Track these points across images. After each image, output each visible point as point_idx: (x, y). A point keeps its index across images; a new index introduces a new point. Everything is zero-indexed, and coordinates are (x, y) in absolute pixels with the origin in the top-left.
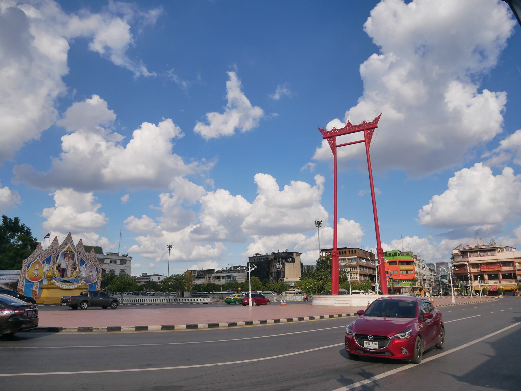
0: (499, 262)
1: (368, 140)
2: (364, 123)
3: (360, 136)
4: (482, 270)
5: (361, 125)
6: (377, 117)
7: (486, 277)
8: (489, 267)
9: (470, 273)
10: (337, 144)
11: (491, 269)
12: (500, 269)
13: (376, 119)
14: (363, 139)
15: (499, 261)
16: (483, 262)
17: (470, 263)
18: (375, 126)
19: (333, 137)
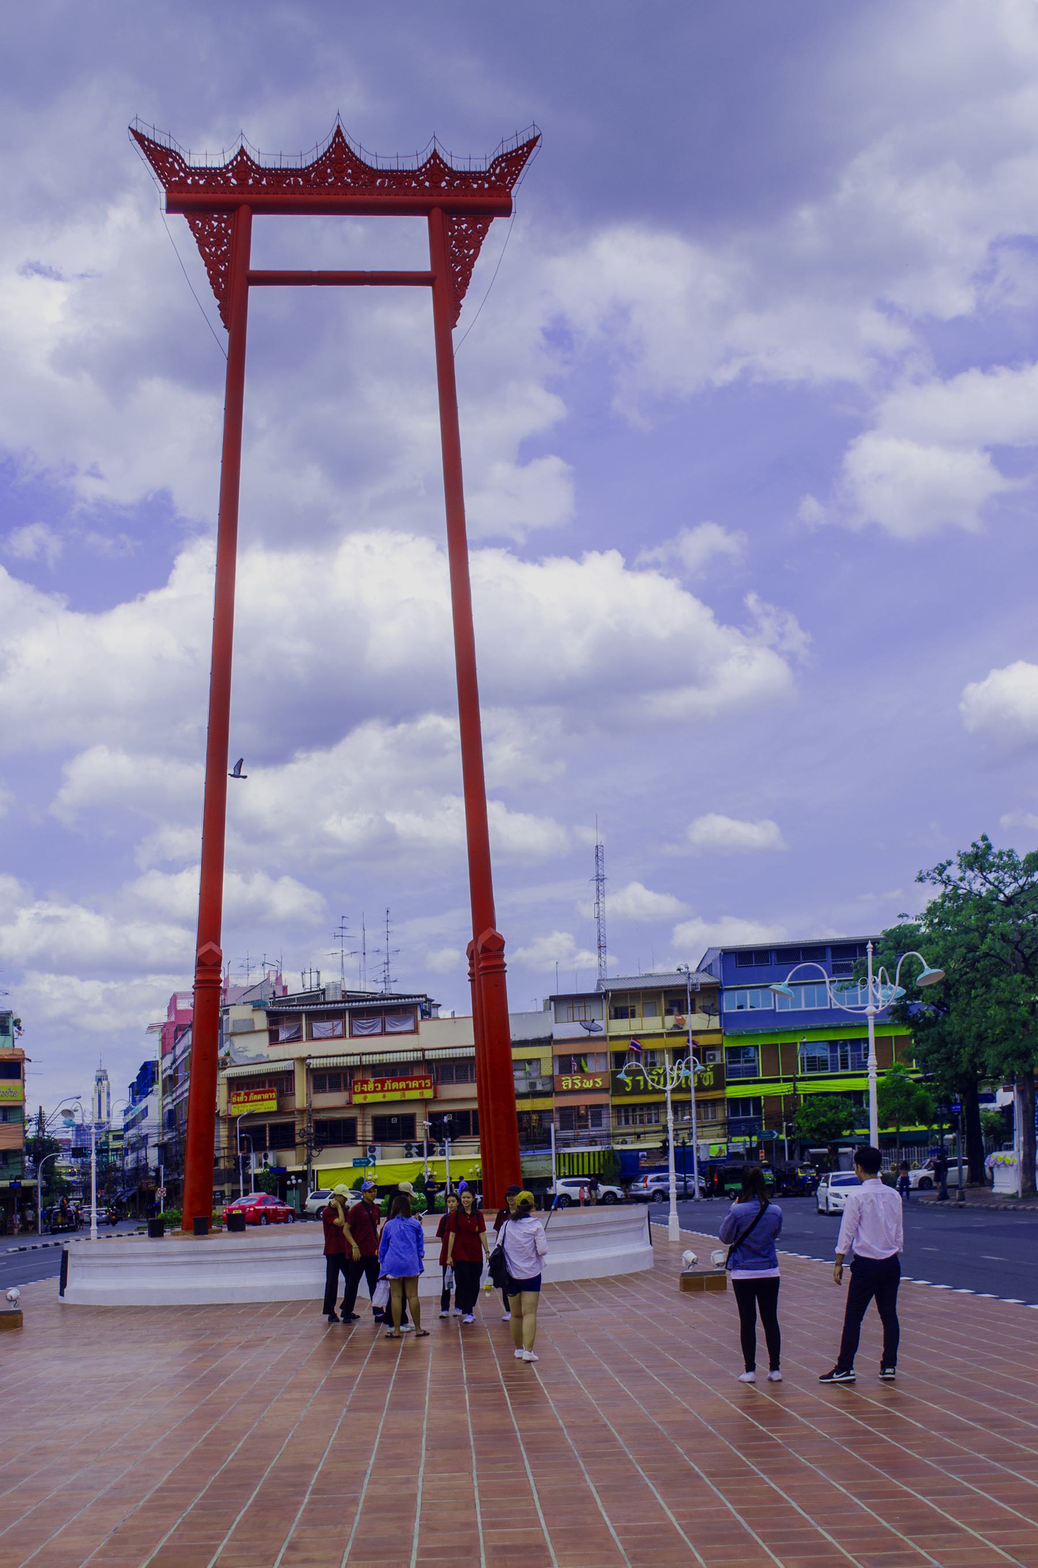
0: (429, 1062)
2: (436, 167)
3: (406, 241)
4: (358, 1099)
5: (412, 175)
7: (365, 1130)
9: (302, 1112)
10: (256, 263)
12: (428, 1094)
15: (429, 1055)
16: (367, 1060)
17: (314, 1063)
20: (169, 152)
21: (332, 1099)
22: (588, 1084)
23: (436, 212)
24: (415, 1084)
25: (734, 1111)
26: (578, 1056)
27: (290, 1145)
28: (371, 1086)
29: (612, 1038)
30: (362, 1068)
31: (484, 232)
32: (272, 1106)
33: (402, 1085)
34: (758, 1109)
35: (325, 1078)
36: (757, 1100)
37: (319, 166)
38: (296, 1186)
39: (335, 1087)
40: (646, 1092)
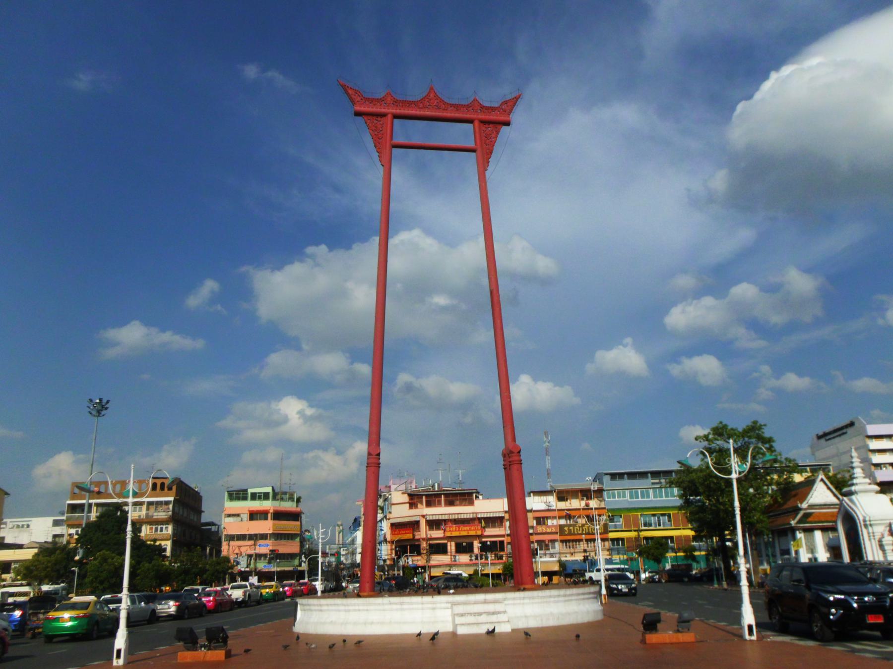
0: (480, 519)
1: (484, 151)
3: (463, 134)
4: (448, 534)
6: (509, 97)
7: (451, 547)
8: (462, 528)
9: (424, 539)
11: (464, 531)
12: (479, 533)
13: (506, 102)
14: (471, 144)
15: (479, 516)
16: (452, 517)
17: (429, 518)
18: (502, 118)
19: (383, 115)
20: (356, 92)
21: (437, 534)
22: (549, 530)
23: (476, 123)
24: (473, 528)
25: (613, 545)
26: (544, 518)
27: (419, 554)
28: (454, 529)
29: (559, 510)
30: (450, 520)
31: (498, 132)
32: (410, 536)
33: (468, 528)
34: (623, 544)
35: (434, 524)
36: (622, 539)
37: (422, 101)
38: (421, 573)
39: (438, 528)
40: (574, 534)
